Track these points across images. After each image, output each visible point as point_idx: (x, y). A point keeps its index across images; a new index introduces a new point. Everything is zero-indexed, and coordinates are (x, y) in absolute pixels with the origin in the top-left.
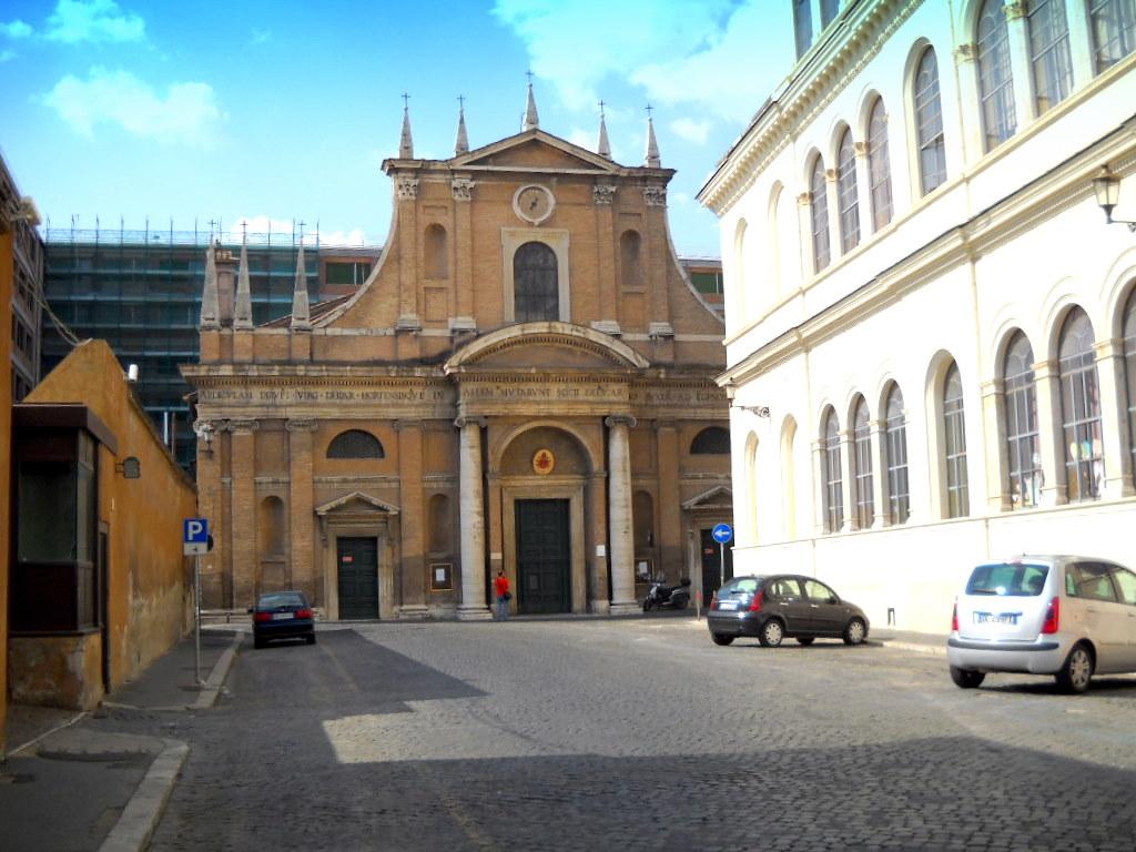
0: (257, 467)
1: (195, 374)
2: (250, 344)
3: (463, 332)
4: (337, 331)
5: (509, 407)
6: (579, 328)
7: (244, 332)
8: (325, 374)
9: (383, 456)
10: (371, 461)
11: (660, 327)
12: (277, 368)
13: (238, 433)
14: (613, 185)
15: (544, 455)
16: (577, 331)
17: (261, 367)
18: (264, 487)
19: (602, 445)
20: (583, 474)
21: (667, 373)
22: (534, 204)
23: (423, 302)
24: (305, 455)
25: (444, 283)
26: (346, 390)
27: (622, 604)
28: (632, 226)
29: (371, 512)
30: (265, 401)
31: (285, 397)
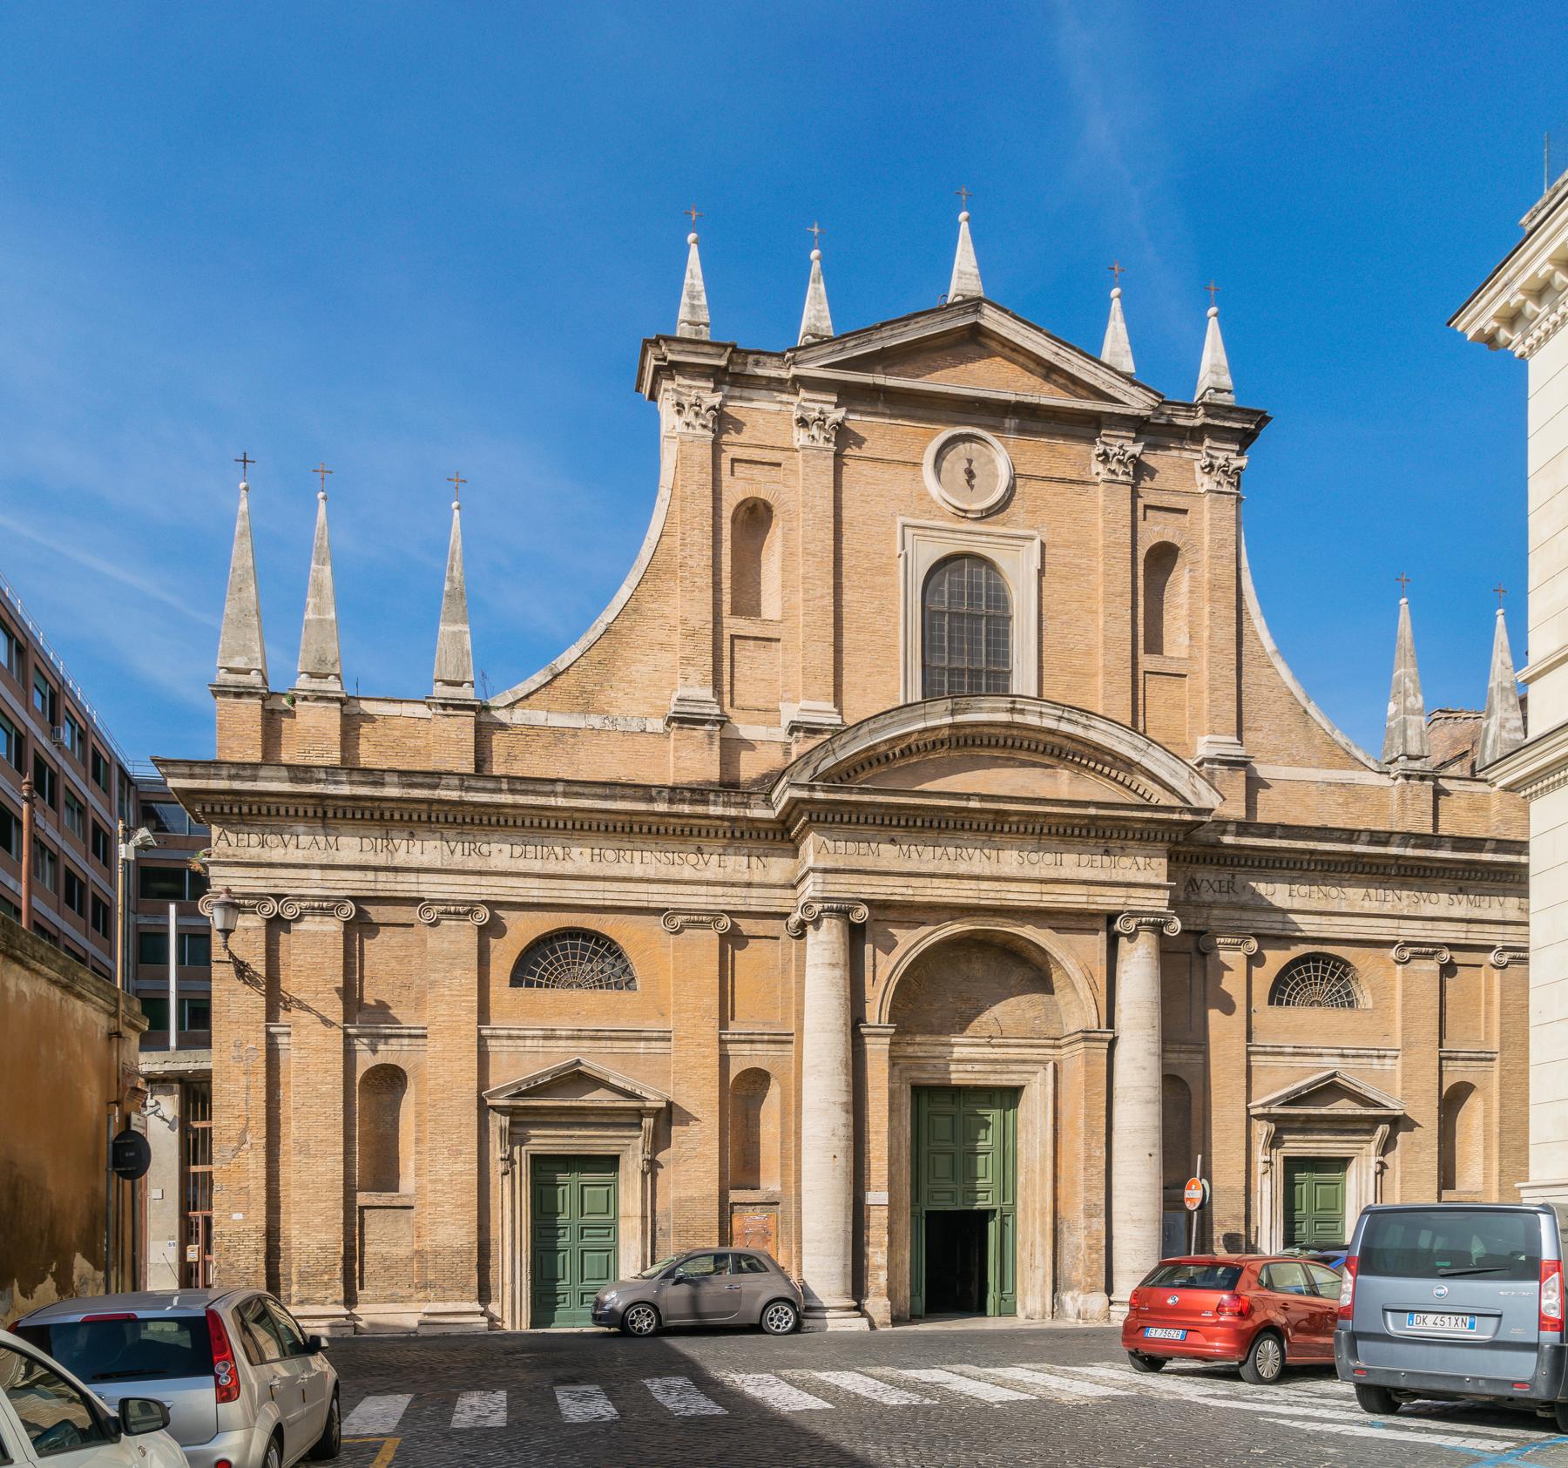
4: (539, 717)
22: (970, 474)
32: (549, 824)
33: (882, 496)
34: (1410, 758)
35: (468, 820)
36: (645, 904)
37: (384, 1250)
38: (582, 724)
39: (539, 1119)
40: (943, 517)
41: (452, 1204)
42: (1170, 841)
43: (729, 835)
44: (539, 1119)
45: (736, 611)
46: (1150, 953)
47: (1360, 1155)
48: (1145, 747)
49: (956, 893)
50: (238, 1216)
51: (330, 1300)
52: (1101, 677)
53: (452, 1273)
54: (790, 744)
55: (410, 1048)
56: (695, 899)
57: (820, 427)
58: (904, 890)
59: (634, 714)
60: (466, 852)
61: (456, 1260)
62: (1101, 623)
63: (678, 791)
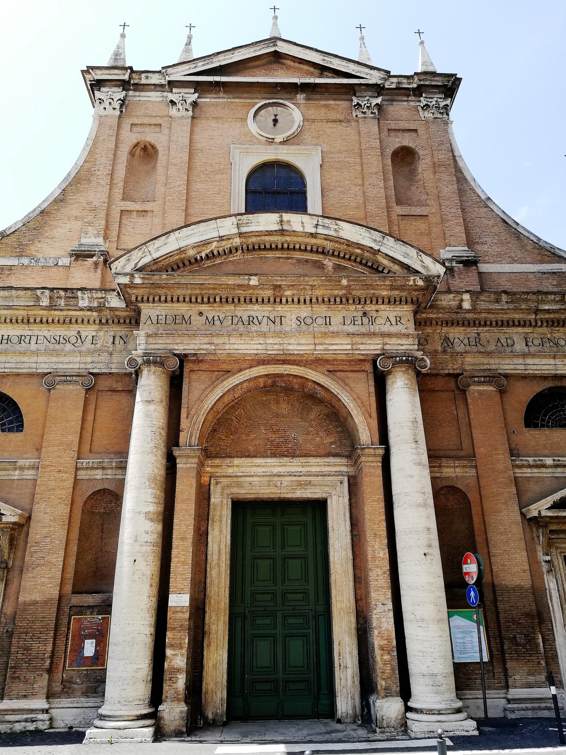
5: (216, 340)
19: (373, 399)
20: (349, 457)
22: (275, 121)
25: (148, 206)
27: (430, 712)
33: (222, 136)
38: (16, 263)
40: (259, 143)
43: (97, 322)
63: (55, 291)
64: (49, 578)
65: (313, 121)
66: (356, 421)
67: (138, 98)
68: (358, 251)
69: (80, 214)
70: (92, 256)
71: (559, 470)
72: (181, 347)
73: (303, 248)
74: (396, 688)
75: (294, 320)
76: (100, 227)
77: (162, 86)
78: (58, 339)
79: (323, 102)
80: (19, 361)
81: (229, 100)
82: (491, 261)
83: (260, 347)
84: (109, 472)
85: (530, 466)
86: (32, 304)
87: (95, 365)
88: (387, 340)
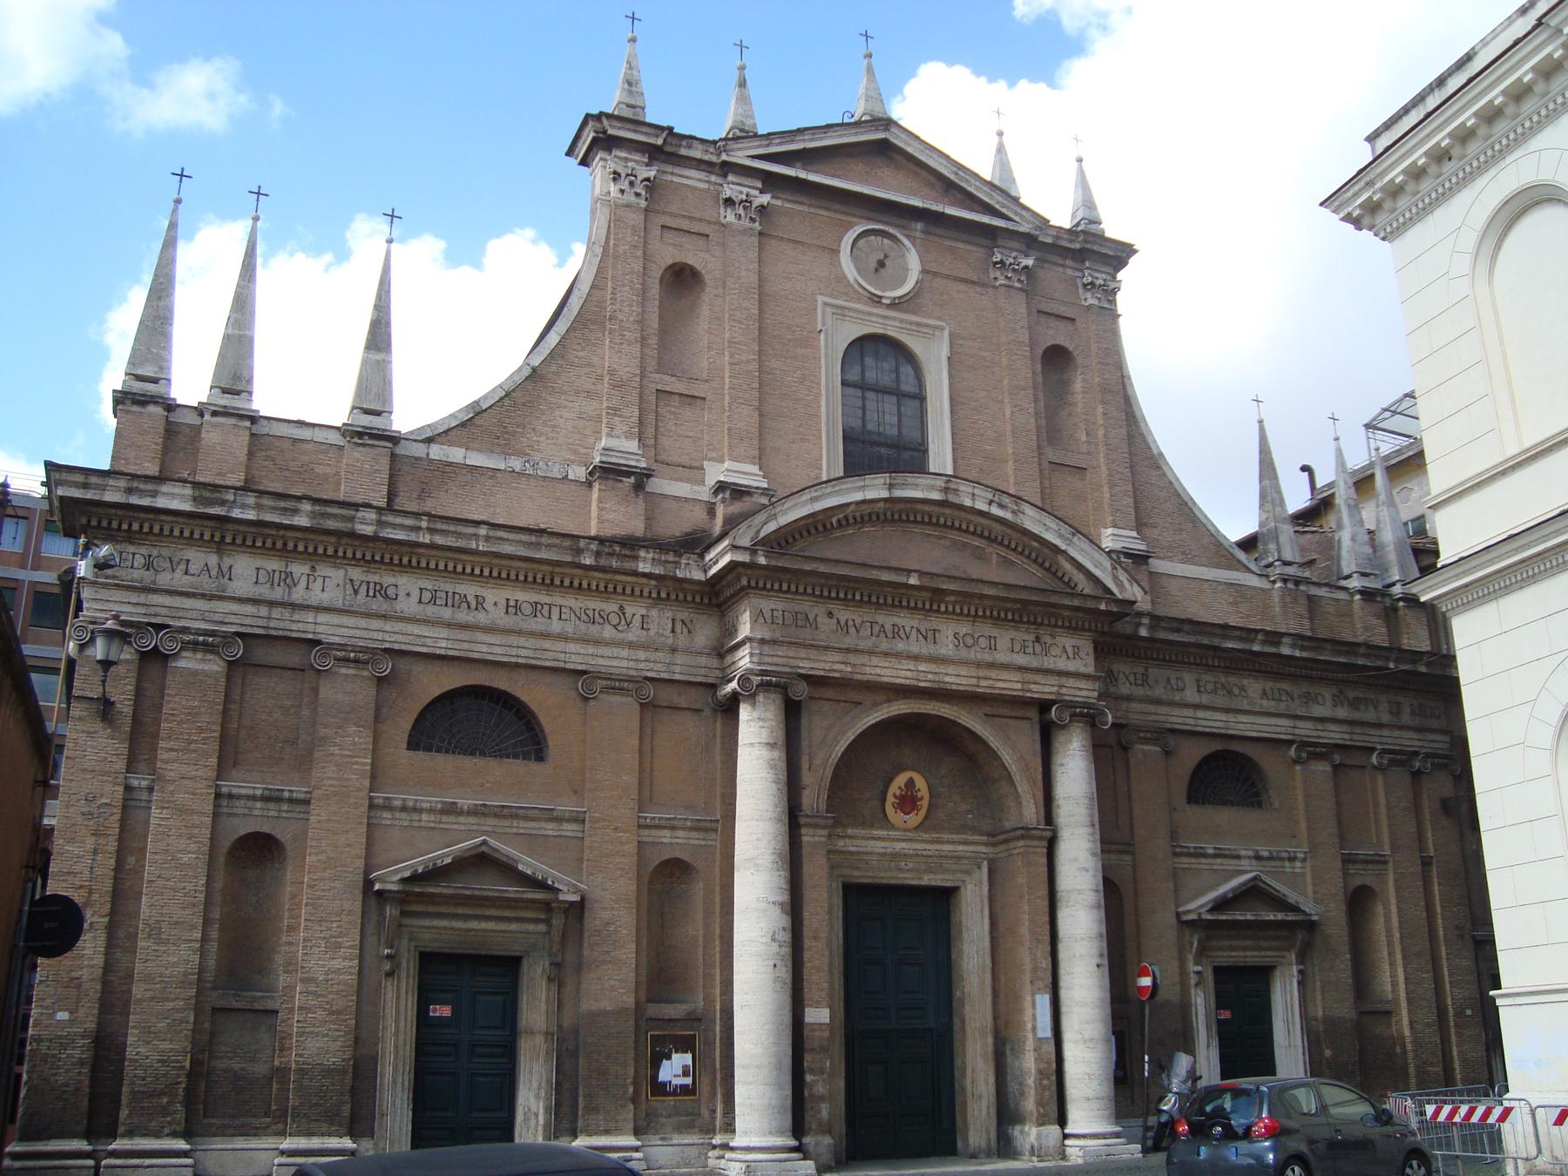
0: (228, 756)
1: (89, 495)
2: (242, 454)
3: (738, 492)
4: (456, 454)
6: (1006, 500)
7: (232, 421)
8: (426, 538)
9: (540, 756)
10: (517, 767)
11: (1125, 538)
12: (307, 507)
13: (188, 662)
14: (1027, 256)
15: (910, 783)
16: (1001, 506)
17: (266, 501)
18: (240, 807)
19: (1039, 760)
21: (1151, 628)
23: (651, 417)
24: (357, 737)
26: (469, 590)
28: (1062, 340)
29: (512, 891)
30: (264, 591)
31: (318, 585)
32: (464, 569)
34: (1286, 564)
35: (377, 558)
36: (562, 665)
37: (237, 1065)
39: (431, 909)
40: (859, 301)
41: (325, 1010)
42: (1096, 631)
44: (431, 909)
45: (661, 369)
46: (1084, 746)
47: (1281, 963)
48: (1070, 536)
49: (894, 673)
50: (62, 1016)
51: (166, 1131)
52: (1010, 463)
53: (321, 1098)
54: (715, 504)
55: (289, 815)
56: (615, 663)
57: (745, 208)
58: (842, 667)
59: (558, 459)
60: (371, 594)
61: (326, 1082)
62: (1008, 413)
64: (618, 980)
65: (935, 274)
66: (1019, 790)
67: (669, 178)
68: (1035, 544)
69: (593, 387)
70: (628, 474)
71: (1219, 861)
72: (807, 664)
73: (964, 527)
74: (1054, 1113)
75: (951, 637)
76: (633, 419)
77: (711, 164)
78: (590, 613)
79: (947, 243)
80: (538, 646)
81: (811, 210)
82: (1161, 555)
83: (909, 674)
84: (680, 833)
85: (1189, 855)
86: (569, 559)
87: (651, 665)
88: (1064, 680)
